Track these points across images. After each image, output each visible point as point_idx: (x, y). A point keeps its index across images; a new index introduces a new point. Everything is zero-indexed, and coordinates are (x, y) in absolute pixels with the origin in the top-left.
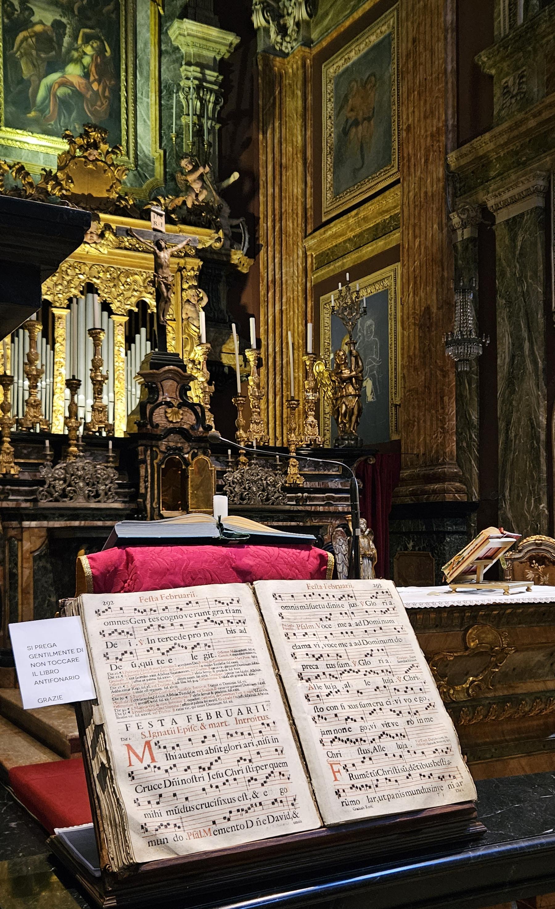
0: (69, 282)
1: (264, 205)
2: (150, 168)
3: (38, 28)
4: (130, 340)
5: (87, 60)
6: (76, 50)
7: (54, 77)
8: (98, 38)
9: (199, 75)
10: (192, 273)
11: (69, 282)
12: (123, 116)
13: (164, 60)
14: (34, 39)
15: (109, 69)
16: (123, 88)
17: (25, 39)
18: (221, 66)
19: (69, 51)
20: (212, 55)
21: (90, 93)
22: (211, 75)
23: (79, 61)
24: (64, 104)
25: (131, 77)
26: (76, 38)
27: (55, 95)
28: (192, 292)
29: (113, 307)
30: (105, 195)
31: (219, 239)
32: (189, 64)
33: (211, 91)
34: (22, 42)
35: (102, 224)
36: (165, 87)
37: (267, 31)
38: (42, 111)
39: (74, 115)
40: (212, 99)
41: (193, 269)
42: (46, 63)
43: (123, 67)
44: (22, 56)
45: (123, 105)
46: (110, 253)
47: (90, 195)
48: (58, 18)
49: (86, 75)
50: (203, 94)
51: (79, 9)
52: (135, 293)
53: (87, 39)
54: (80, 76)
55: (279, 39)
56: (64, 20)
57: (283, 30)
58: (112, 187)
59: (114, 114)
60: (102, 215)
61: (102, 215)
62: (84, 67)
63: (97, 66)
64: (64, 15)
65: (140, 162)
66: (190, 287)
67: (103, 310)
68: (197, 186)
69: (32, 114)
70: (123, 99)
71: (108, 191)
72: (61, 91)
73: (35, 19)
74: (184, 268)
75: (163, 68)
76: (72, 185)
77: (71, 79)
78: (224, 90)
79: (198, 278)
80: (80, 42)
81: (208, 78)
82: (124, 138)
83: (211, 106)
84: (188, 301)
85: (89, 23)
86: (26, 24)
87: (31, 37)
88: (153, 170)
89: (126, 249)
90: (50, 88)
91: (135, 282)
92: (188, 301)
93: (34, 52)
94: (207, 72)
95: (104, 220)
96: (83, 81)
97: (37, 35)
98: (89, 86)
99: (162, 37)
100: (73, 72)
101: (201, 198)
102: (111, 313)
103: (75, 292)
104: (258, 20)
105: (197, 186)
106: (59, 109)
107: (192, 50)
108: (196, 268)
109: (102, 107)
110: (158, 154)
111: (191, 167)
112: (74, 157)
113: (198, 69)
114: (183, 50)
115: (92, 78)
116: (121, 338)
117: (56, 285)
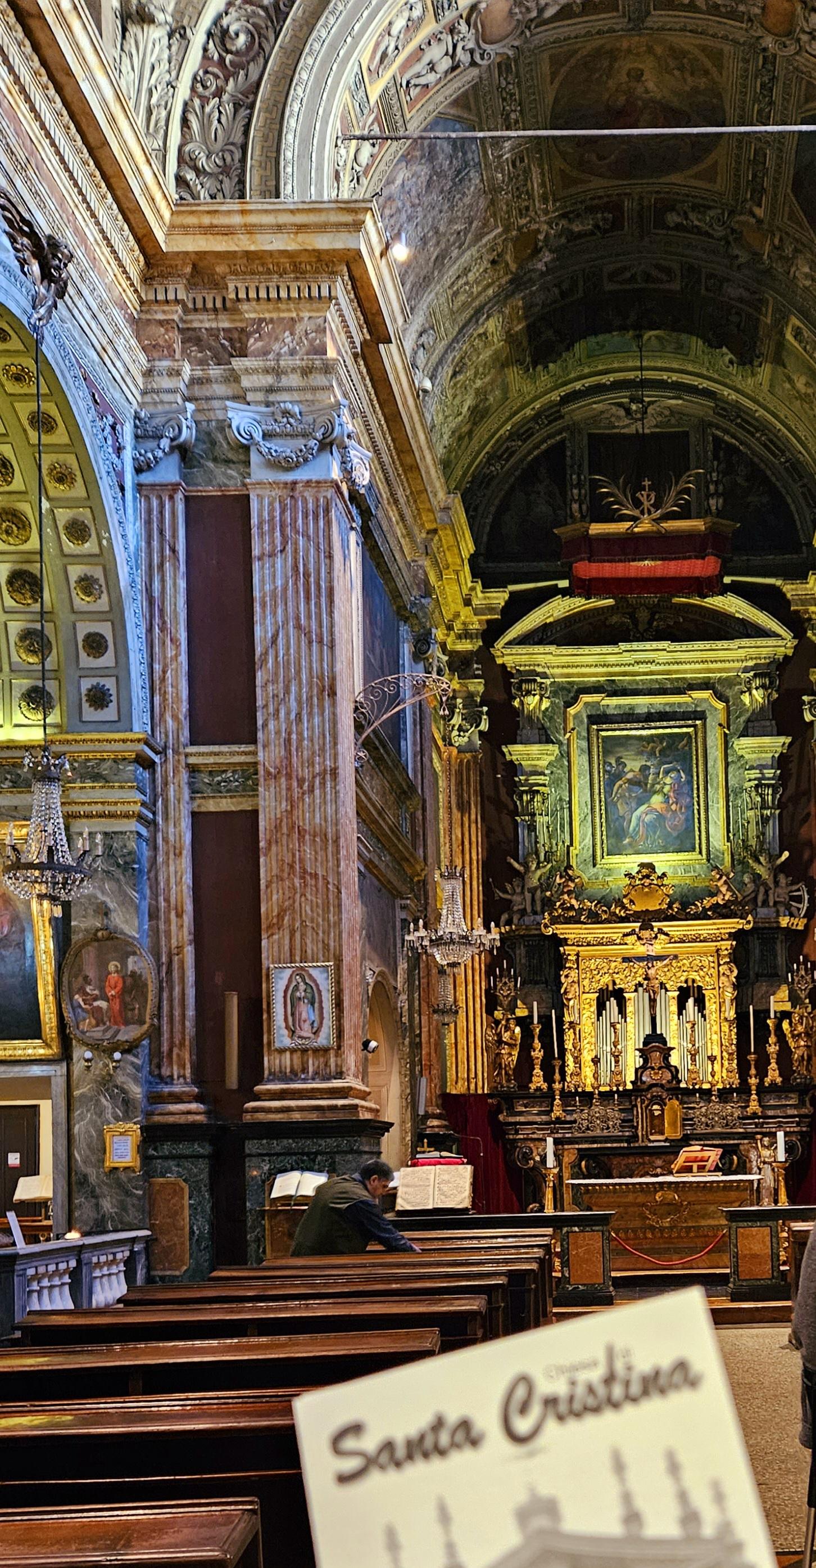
3: (630, 776)
7: (643, 808)
8: (674, 769)
13: (730, 769)
15: (685, 790)
19: (653, 785)
22: (769, 773)
23: (661, 791)
24: (649, 826)
32: (752, 768)
33: (768, 786)
49: (667, 801)
53: (667, 772)
69: (627, 841)
100: (656, 800)
103: (640, 979)
114: (747, 757)
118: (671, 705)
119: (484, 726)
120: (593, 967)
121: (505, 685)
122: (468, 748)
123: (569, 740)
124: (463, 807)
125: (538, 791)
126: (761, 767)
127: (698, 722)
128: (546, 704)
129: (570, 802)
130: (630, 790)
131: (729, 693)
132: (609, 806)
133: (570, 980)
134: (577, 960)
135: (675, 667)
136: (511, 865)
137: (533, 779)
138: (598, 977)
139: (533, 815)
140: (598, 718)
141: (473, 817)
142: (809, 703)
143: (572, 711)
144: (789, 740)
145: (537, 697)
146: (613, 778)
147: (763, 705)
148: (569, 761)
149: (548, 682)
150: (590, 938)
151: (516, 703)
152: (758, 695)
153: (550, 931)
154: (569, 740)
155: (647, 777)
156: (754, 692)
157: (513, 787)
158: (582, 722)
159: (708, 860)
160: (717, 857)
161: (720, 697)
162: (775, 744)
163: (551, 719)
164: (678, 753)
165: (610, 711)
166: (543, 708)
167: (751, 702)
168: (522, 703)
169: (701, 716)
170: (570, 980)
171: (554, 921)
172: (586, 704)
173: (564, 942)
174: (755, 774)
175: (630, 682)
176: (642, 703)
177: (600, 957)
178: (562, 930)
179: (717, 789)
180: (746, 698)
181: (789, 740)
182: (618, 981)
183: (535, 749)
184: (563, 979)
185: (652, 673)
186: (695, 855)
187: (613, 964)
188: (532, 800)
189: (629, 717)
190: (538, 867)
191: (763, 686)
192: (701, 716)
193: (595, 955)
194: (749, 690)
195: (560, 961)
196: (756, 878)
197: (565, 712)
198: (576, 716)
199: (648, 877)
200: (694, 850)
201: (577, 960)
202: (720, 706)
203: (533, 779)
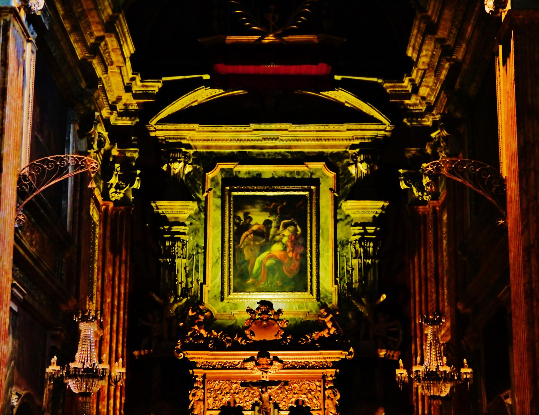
0: (253, 393)
2: (329, 298)
3: (255, 228)
5: (285, 240)
6: (279, 234)
7: (265, 254)
9: (363, 231)
10: (331, 379)
11: (253, 393)
12: (309, 270)
13: (339, 225)
14: (252, 235)
15: (299, 241)
16: (308, 252)
17: (247, 236)
19: (274, 236)
20: (372, 215)
21: (287, 259)
22: (370, 229)
23: (280, 241)
24: (271, 270)
25: (314, 243)
26: (278, 227)
27: (264, 265)
28: (330, 391)
29: (281, 406)
30: (274, 338)
31: (350, 354)
32: (356, 225)
33: (370, 240)
34: (245, 238)
35: (271, 357)
36: (340, 243)
37: (412, 190)
38: (256, 278)
39: (277, 275)
40: (371, 244)
41: (331, 376)
42: (259, 247)
43: (309, 238)
44: (244, 247)
45: (309, 262)
46: (276, 373)
47: (265, 340)
48: (267, 218)
49: (285, 249)
50: (364, 244)
51: (280, 209)
52: (295, 396)
53: (286, 226)
54: (280, 251)
55: (420, 194)
56: (271, 219)
57: (421, 189)
58: (278, 333)
59: (302, 270)
60: (270, 352)
61: (270, 352)
62: (283, 244)
63: (291, 241)
64: (271, 215)
65: (322, 296)
66: (330, 388)
67: (275, 408)
68: (329, 325)
69: (250, 281)
70: (308, 259)
71: (276, 336)
73: (252, 223)
74: (326, 375)
75: (338, 231)
76: (253, 337)
77: (274, 254)
79: (333, 381)
80: (281, 229)
81: (369, 231)
82: (309, 283)
83: (371, 249)
84: (329, 397)
85: (287, 216)
86: (247, 227)
87: (251, 234)
88: (331, 299)
89: (288, 368)
90: (262, 263)
91: (295, 388)
92: (329, 397)
93: (252, 243)
94: (367, 228)
95: (272, 354)
96: (283, 253)
97: (254, 232)
98: (286, 256)
99: (338, 211)
100: (276, 249)
101: (332, 332)
102: (280, 410)
104: (403, 186)
105: (329, 325)
106: (268, 274)
107: (358, 215)
108: (333, 374)
110: (334, 288)
111: (325, 314)
112: (254, 320)
113: (361, 228)
114: (353, 216)
115: (288, 250)
117: (245, 397)
118: (291, 173)
119: (137, 185)
120: (217, 387)
123: (206, 198)
124: (116, 251)
125: (179, 239)
126: (364, 225)
127: (313, 187)
128: (189, 169)
129: (205, 248)
130: (254, 240)
131: (340, 164)
132: (238, 251)
133: (196, 398)
134: (203, 382)
135: (295, 143)
136: (153, 299)
137: (175, 229)
138: (220, 397)
139: (174, 258)
140: (230, 180)
141: (124, 258)
142: (404, 174)
143: (210, 175)
145: (182, 164)
146: (241, 228)
147: (367, 175)
148: (206, 215)
149: (191, 151)
150: (215, 362)
151: (165, 168)
152: (363, 167)
154: (206, 198)
155: (269, 229)
156: (359, 164)
157: (159, 237)
158: (217, 184)
159: (318, 299)
160: (327, 297)
161: (331, 167)
163: (193, 181)
164: (297, 211)
165: (241, 176)
166: (186, 172)
167: (357, 174)
168: (169, 168)
170: (196, 398)
172: (222, 170)
173: (194, 365)
174: (359, 230)
175: (258, 154)
176: (267, 171)
177: (223, 379)
178: (192, 355)
179: (327, 241)
180: (352, 169)
181: (386, 204)
182: (238, 400)
183: (178, 204)
184: (191, 398)
185: (276, 147)
186: (306, 295)
187: (234, 386)
188: (173, 245)
189: (257, 181)
190: (175, 301)
192: (317, 182)
194: (356, 163)
195: (190, 381)
197: (204, 177)
198: (213, 180)
199: (266, 312)
200: (305, 290)
201: (203, 382)
202: (331, 175)
203: (175, 229)
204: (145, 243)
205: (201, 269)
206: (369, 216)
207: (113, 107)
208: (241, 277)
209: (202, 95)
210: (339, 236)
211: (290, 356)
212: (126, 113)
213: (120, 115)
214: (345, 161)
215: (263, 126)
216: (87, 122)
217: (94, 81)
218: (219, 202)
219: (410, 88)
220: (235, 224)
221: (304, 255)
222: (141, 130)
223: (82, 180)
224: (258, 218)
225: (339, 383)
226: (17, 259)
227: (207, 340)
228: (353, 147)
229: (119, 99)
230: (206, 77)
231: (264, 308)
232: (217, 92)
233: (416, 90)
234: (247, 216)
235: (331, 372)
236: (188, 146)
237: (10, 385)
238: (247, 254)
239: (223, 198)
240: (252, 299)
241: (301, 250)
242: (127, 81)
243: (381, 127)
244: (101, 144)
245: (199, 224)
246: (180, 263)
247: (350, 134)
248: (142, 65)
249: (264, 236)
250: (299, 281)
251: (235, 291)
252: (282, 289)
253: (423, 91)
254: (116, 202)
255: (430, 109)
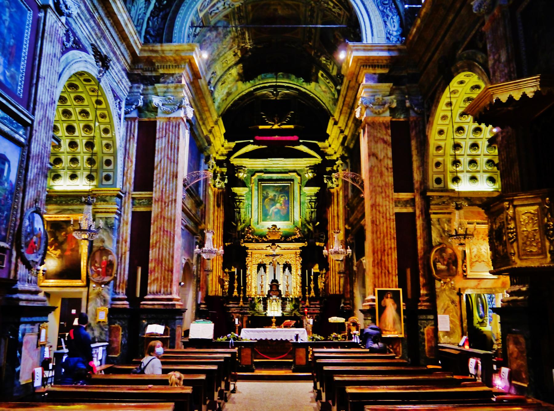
1: (330, 227)
3: (270, 197)
4: (284, 270)
5: (281, 202)
7: (274, 207)
13: (302, 196)
15: (287, 203)
18: (316, 195)
22: (313, 198)
38: (270, 216)
49: (281, 205)
53: (282, 197)
57: (332, 183)
68: (298, 234)
69: (268, 217)
72: (276, 210)
78: (316, 201)
79: (300, 254)
90: (272, 210)
98: (282, 208)
100: (278, 205)
104: (325, 182)
105: (298, 234)
109: (285, 211)
116: (282, 270)
119: (226, 181)
121: (233, 169)
122: (221, 188)
124: (219, 206)
126: (311, 196)
128: (245, 175)
131: (301, 174)
132: (264, 206)
137: (240, 198)
139: (240, 209)
140: (261, 180)
143: (253, 178)
144: (319, 188)
146: (265, 198)
147: (312, 179)
149: (246, 169)
150: (256, 247)
151: (236, 175)
153: (243, 245)
155: (275, 198)
157: (234, 201)
162: (315, 190)
163: (247, 180)
164: (286, 191)
169: (292, 180)
171: (245, 242)
173: (248, 248)
174: (309, 198)
176: (275, 176)
178: (247, 245)
180: (307, 175)
181: (319, 188)
183: (241, 189)
186: (289, 222)
191: (312, 172)
193: (257, 253)
195: (246, 255)
196: (309, 230)
198: (254, 179)
199: (274, 229)
200: (289, 220)
202: (299, 177)
203: (240, 198)
204: (229, 203)
205: (250, 213)
206: (313, 193)
207: (217, 153)
208: (265, 215)
209: (250, 148)
210: (302, 201)
211: (283, 245)
212: (222, 155)
213: (220, 155)
214: (304, 172)
215: (273, 159)
216: (208, 158)
217: (210, 143)
218: (257, 188)
219: (328, 145)
220: (263, 196)
221: (288, 208)
222: (227, 161)
223: (206, 180)
224: (271, 194)
225: (301, 255)
226: (183, 210)
227: (253, 239)
228: (307, 167)
229: (219, 149)
230: (252, 141)
231: (274, 227)
232: (256, 147)
233: (330, 146)
234: (267, 194)
235: (299, 251)
236: (245, 167)
237: (182, 255)
238: (267, 207)
239: (258, 186)
240: (269, 224)
241: (287, 206)
242: (222, 143)
243: (318, 160)
244: (213, 167)
245: (250, 196)
246: (242, 211)
247: (305, 162)
248: (228, 137)
249: (273, 201)
250: (286, 217)
251: (263, 221)
252: (280, 220)
253: (332, 146)
254: (219, 189)
255: (335, 153)
